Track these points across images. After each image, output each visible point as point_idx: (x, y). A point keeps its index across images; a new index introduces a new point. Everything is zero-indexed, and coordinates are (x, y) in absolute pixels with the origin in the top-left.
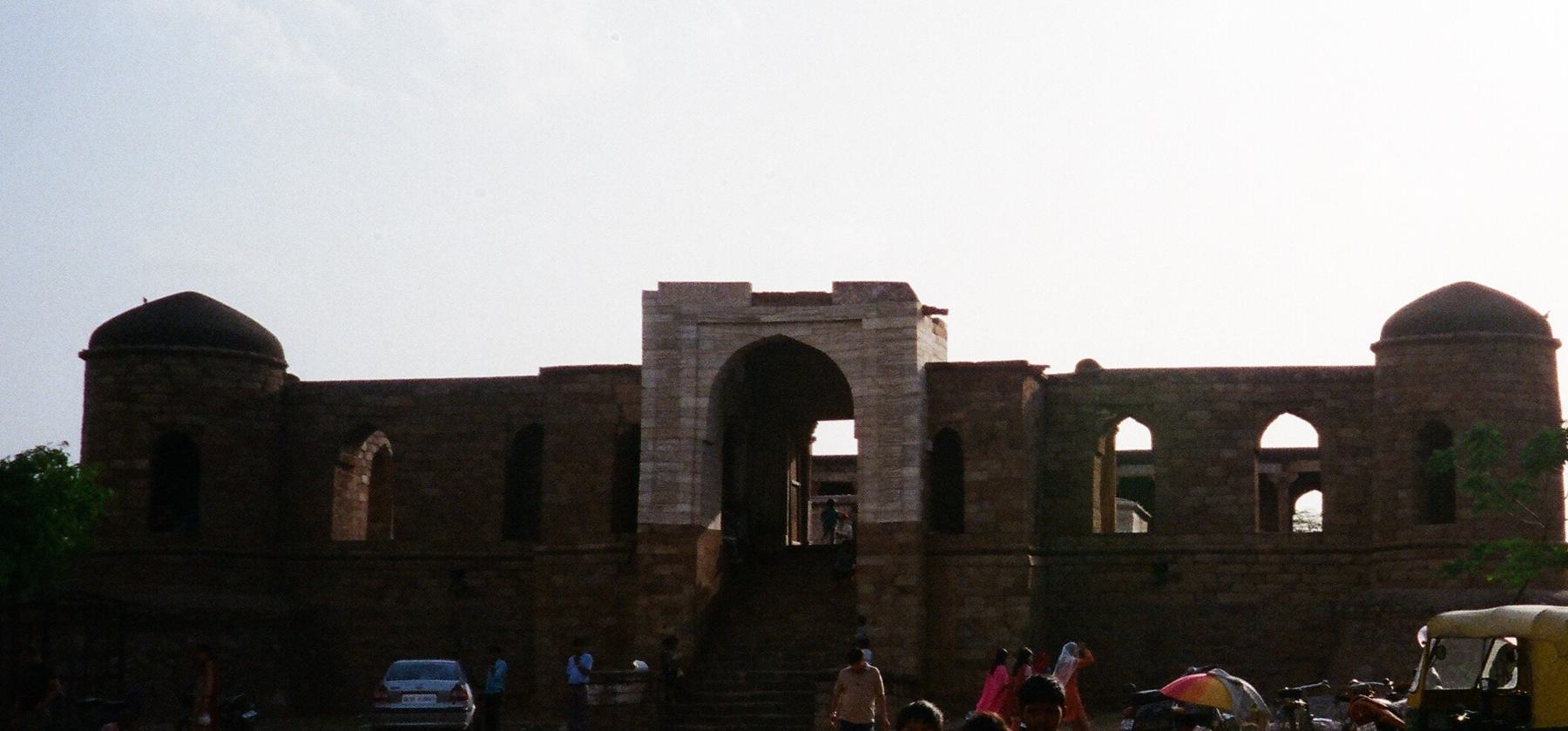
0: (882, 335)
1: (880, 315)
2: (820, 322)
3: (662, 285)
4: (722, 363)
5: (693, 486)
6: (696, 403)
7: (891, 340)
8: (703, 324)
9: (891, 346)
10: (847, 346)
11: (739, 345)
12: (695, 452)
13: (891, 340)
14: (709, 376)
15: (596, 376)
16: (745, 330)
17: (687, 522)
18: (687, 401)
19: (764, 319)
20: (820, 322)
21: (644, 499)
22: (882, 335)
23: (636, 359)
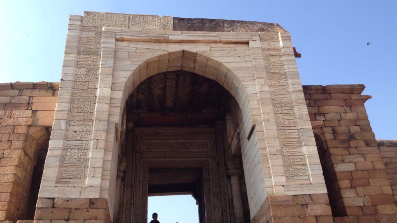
0: (268, 53)
1: (261, 39)
2: (215, 42)
3: (87, 13)
4: (134, 67)
5: (104, 161)
6: (108, 96)
7: (272, 56)
8: (122, 40)
9: (273, 60)
10: (239, 59)
11: (150, 56)
12: (108, 133)
13: (272, 56)
14: (126, 75)
15: (16, 92)
16: (157, 46)
17: (94, 195)
18: (102, 90)
19: (171, 38)
20: (215, 42)
21: (50, 171)
22: (268, 53)
23: (54, 76)
